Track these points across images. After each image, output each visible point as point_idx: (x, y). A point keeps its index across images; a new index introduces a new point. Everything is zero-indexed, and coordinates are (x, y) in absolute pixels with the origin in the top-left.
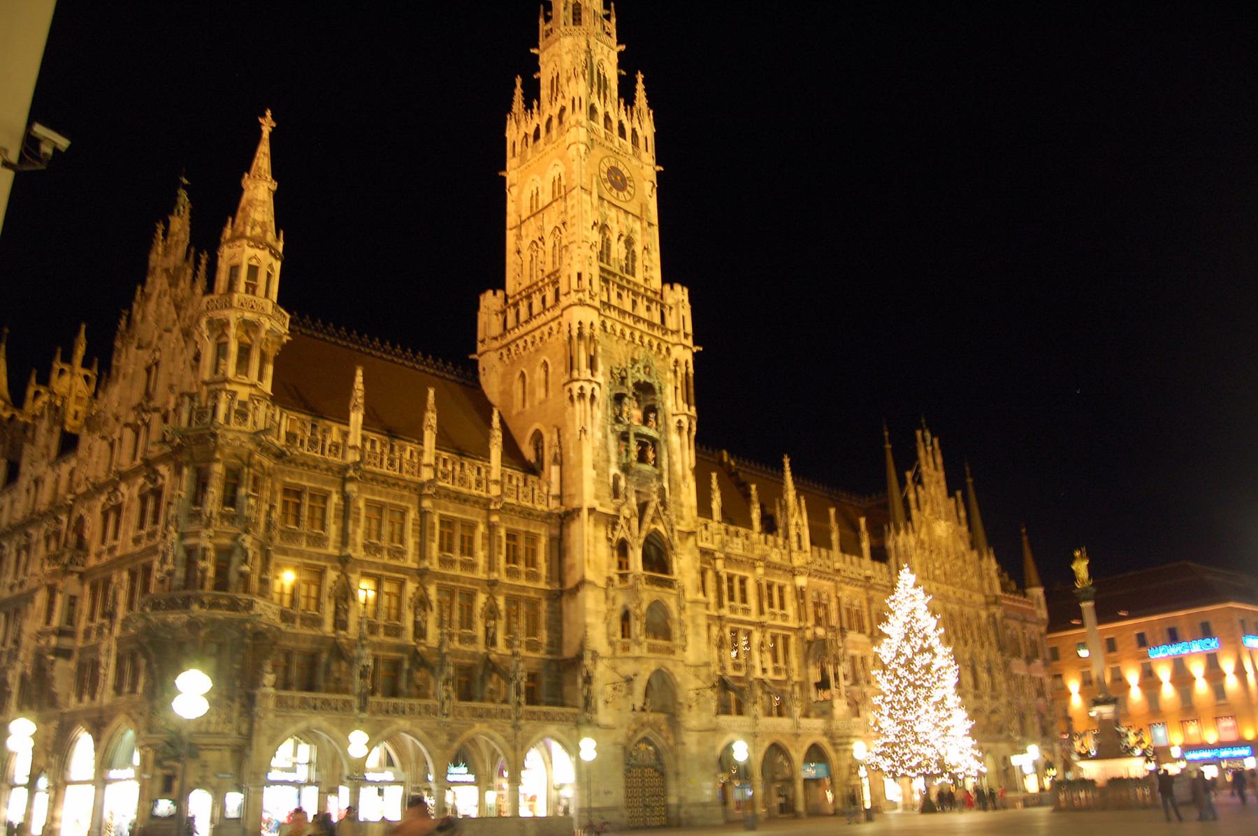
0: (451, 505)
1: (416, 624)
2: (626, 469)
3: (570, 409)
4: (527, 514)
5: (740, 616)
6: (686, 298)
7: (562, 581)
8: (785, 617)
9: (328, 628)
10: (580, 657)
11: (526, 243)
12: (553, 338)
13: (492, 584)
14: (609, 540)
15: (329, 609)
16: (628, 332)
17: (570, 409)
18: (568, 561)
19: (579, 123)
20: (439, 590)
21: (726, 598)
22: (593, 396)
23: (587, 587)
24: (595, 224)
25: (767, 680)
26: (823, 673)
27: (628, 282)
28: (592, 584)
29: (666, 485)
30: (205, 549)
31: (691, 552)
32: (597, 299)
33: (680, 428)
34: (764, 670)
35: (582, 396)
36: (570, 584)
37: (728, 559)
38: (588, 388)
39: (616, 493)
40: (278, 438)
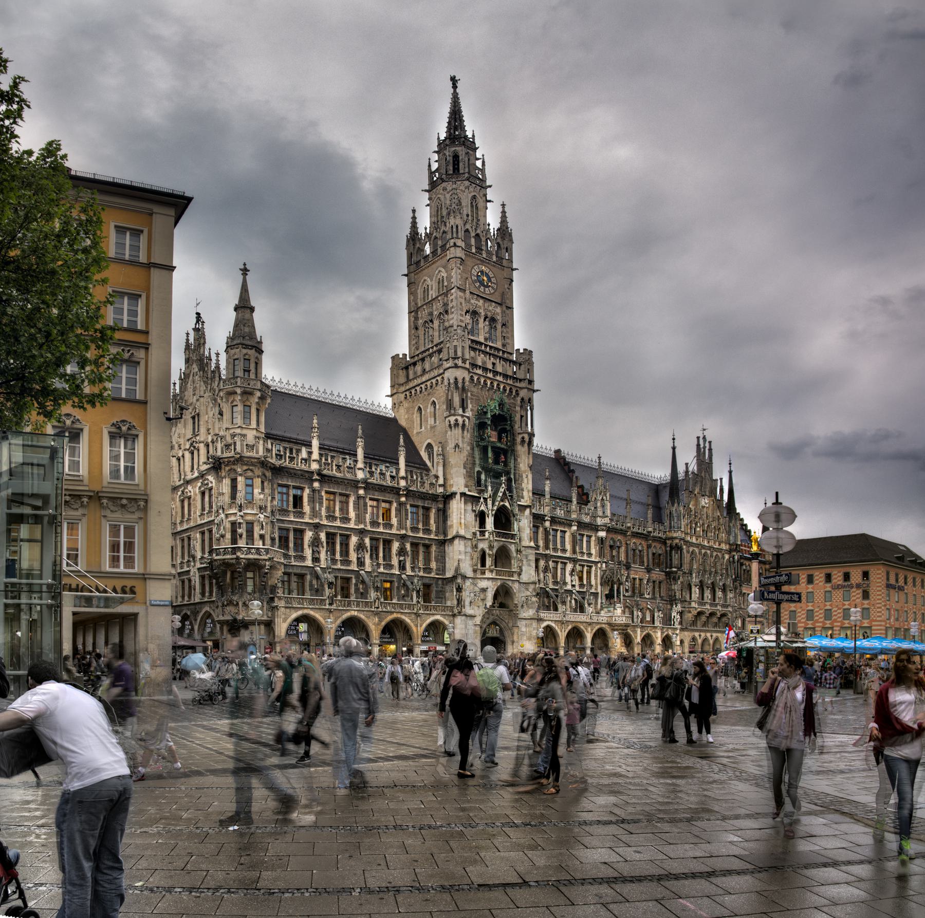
0: (376, 493)
1: (358, 559)
3: (449, 433)
4: (424, 496)
5: (559, 554)
7: (445, 534)
8: (590, 555)
9: (309, 563)
12: (438, 387)
13: (403, 537)
15: (308, 552)
17: (449, 433)
18: (449, 523)
20: (371, 539)
22: (464, 425)
24: (467, 312)
26: (612, 590)
28: (464, 538)
35: (456, 425)
37: (554, 520)
38: (460, 420)
39: (479, 483)
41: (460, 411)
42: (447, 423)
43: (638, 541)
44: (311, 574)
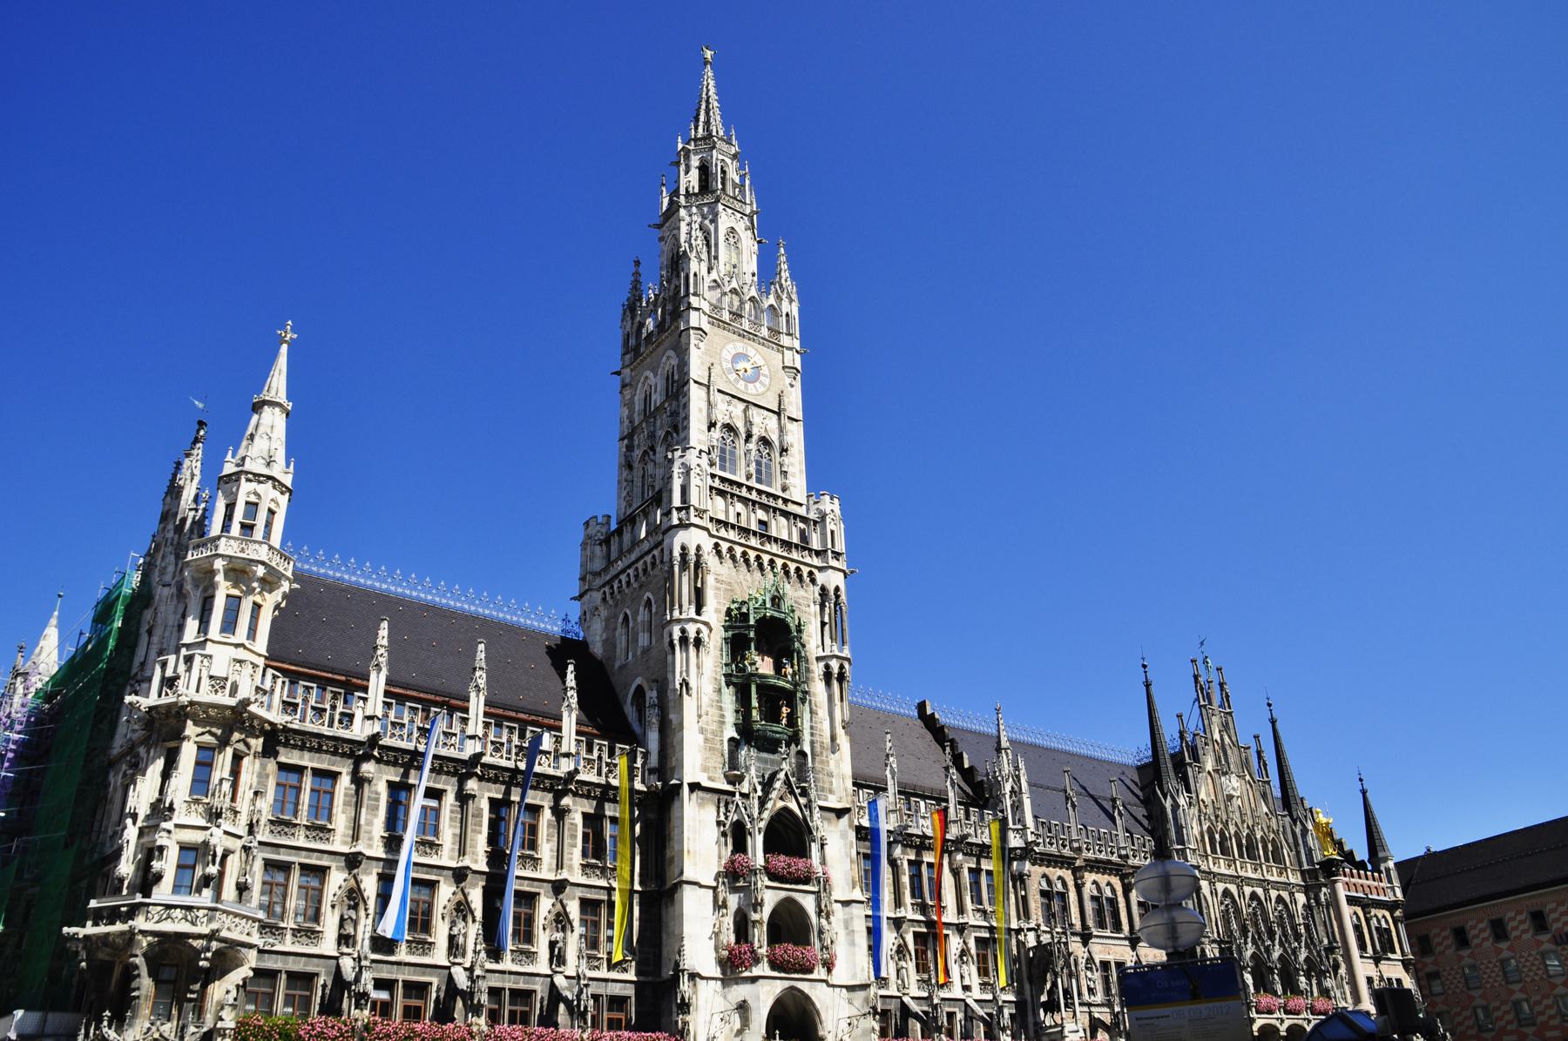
1: (452, 938)
2: (747, 734)
6: (836, 506)
10: (675, 981)
11: (638, 453)
12: (656, 572)
13: (559, 887)
14: (719, 823)
15: (330, 924)
16: (752, 555)
17: (670, 657)
18: (668, 854)
19: (689, 307)
21: (907, 893)
22: (698, 642)
23: (685, 887)
24: (712, 425)
25: (970, 1001)
27: (760, 492)
29: (807, 749)
30: (161, 849)
31: (844, 836)
32: (706, 516)
33: (828, 676)
34: (966, 988)
35: (684, 640)
36: (668, 885)
38: (691, 630)
39: (733, 762)
40: (269, 707)
41: (693, 614)
42: (667, 640)
43: (1103, 879)
44: (327, 974)
